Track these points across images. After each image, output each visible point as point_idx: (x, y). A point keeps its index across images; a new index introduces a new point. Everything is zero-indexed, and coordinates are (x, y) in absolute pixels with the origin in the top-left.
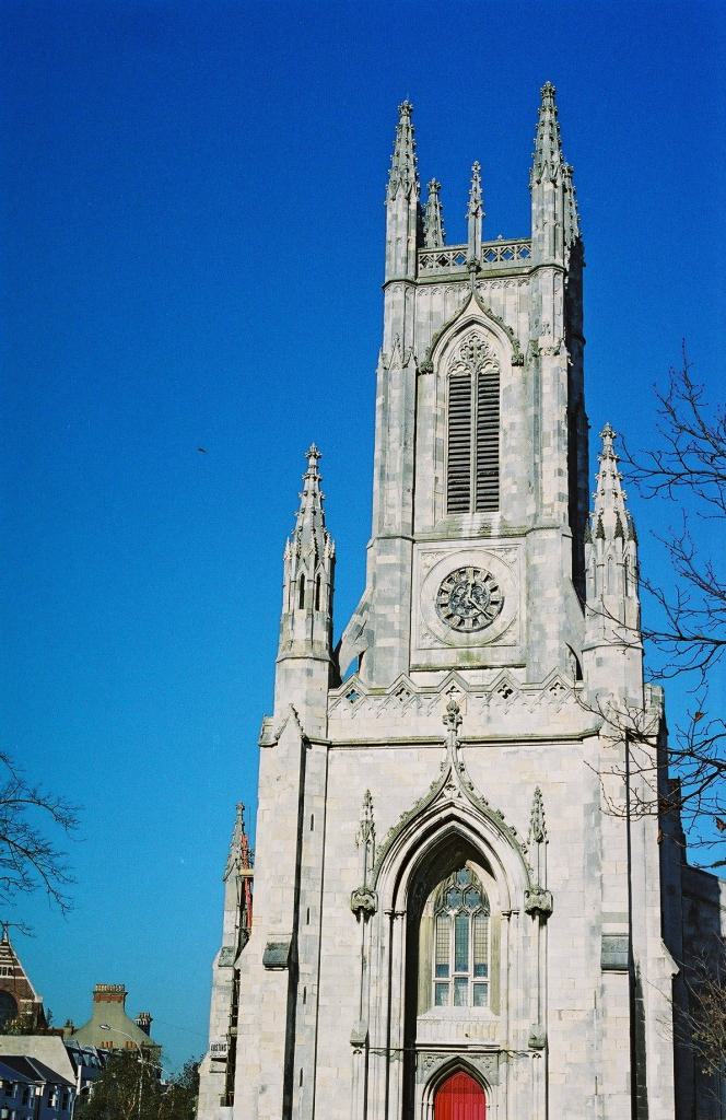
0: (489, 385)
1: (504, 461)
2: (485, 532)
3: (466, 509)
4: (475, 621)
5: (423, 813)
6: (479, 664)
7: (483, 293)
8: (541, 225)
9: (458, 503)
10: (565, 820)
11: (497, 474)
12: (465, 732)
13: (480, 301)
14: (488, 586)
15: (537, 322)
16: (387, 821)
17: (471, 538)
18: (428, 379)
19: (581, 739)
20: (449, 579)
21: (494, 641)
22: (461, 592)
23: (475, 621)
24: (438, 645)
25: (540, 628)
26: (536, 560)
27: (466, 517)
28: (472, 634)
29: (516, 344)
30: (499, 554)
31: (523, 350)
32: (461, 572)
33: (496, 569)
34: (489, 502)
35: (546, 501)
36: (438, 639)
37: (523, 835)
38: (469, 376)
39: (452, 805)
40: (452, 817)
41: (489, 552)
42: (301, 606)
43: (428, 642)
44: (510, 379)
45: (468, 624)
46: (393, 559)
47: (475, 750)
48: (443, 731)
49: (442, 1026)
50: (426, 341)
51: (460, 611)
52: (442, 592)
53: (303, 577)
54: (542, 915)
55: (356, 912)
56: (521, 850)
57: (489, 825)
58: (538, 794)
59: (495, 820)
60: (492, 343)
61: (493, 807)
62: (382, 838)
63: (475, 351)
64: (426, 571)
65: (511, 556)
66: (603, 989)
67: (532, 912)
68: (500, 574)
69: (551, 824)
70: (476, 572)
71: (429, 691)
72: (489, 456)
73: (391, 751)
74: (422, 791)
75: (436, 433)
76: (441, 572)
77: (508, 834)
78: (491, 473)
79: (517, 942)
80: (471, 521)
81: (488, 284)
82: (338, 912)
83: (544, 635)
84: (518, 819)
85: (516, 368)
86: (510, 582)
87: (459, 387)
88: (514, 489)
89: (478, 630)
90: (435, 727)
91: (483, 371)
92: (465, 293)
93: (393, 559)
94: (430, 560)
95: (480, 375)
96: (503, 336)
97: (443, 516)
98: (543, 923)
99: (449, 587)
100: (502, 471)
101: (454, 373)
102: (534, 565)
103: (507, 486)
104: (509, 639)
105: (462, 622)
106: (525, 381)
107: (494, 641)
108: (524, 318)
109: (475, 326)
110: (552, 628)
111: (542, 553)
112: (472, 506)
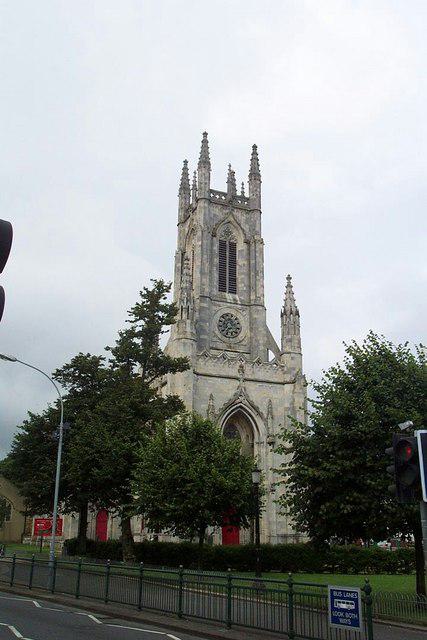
0: (233, 247)
5: (231, 404)
9: (222, 288)
16: (219, 404)
19: (284, 384)
20: (222, 317)
34: (233, 291)
40: (241, 407)
44: (241, 246)
56: (265, 421)
59: (256, 409)
61: (255, 404)
62: (217, 412)
63: (228, 233)
69: (275, 413)
71: (233, 359)
72: (233, 273)
73: (219, 379)
74: (230, 394)
75: (216, 260)
76: (219, 314)
77: (260, 414)
78: (233, 280)
80: (229, 296)
84: (263, 410)
87: (222, 245)
90: (234, 372)
93: (205, 305)
96: (241, 231)
103: (241, 286)
106: (249, 250)
108: (247, 226)
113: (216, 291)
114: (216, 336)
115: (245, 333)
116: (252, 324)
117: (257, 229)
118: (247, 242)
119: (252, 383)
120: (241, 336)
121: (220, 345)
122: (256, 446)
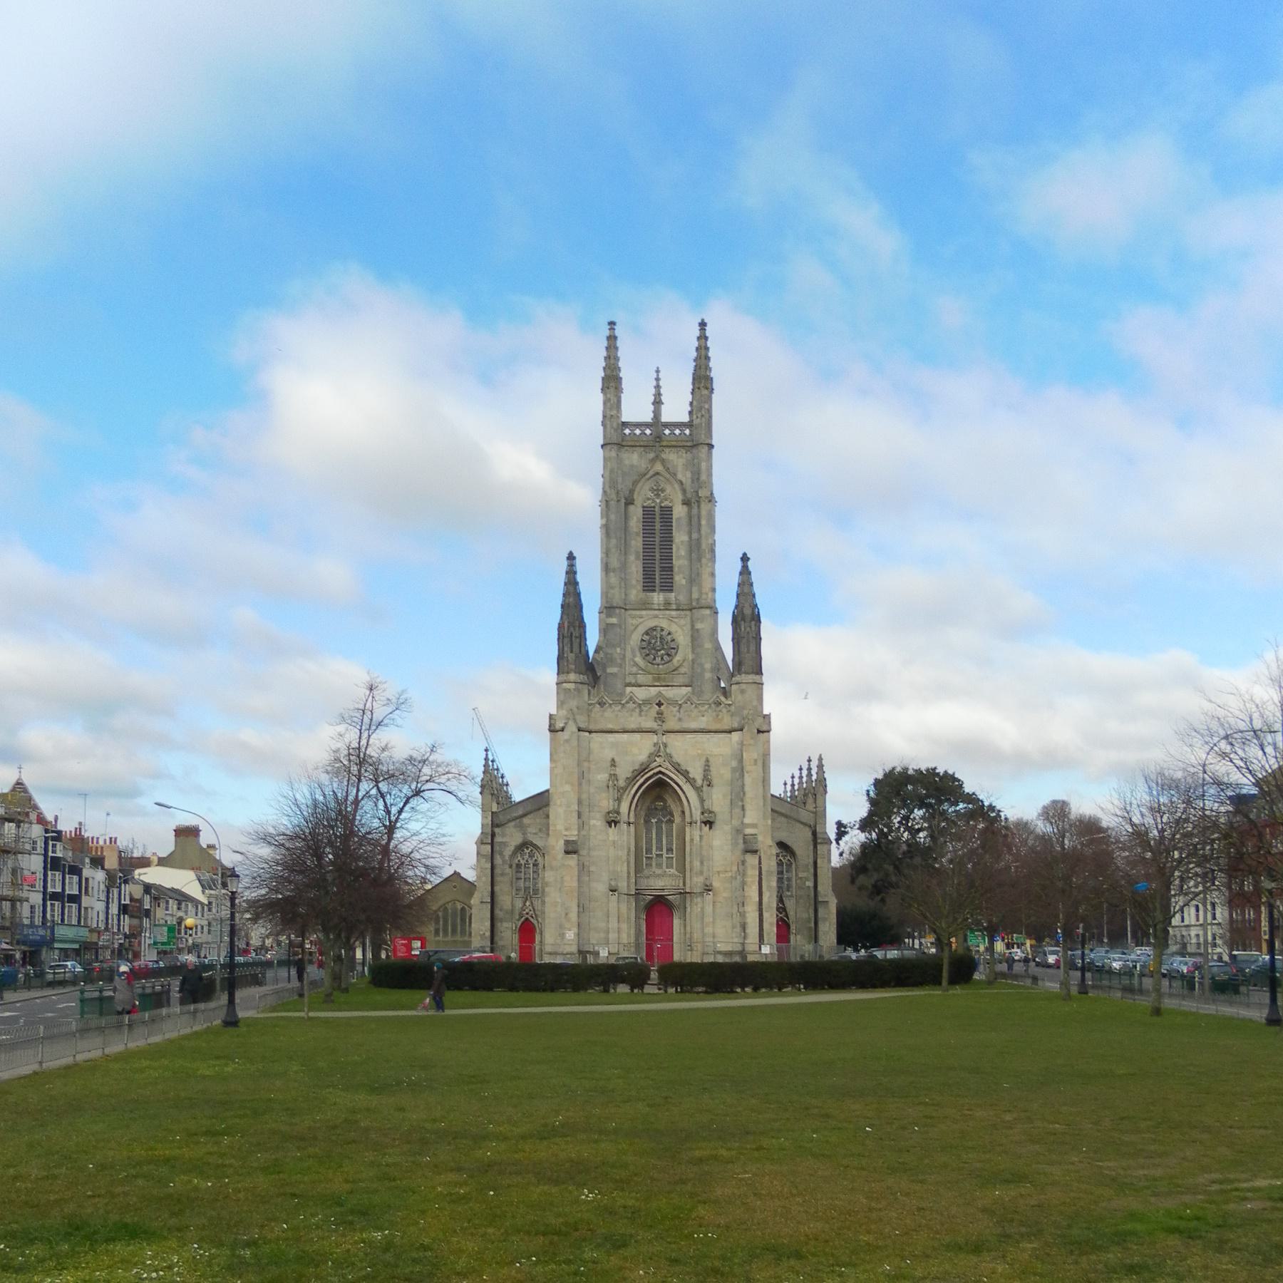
0: (667, 513)
1: (676, 563)
2: (667, 606)
3: (654, 591)
4: (662, 659)
5: (643, 769)
6: (664, 684)
7: (663, 456)
8: (699, 416)
9: (649, 586)
10: (722, 774)
11: (672, 571)
12: (665, 727)
13: (663, 462)
14: (669, 637)
15: (698, 479)
16: (624, 772)
17: (660, 610)
18: (631, 508)
20: (647, 633)
21: (673, 671)
22: (653, 641)
23: (662, 659)
24: (640, 672)
25: (701, 665)
26: (699, 626)
27: (655, 594)
28: (661, 666)
29: (684, 491)
30: (676, 620)
31: (689, 495)
32: (654, 629)
33: (674, 628)
34: (668, 586)
35: (704, 591)
36: (642, 670)
37: (699, 782)
38: (654, 507)
39: (660, 766)
40: (660, 772)
41: (670, 619)
42: (572, 652)
43: (634, 669)
44: (679, 511)
45: (658, 660)
46: (614, 620)
47: (672, 735)
48: (654, 725)
49: (662, 881)
50: (629, 484)
51: (653, 652)
52: (643, 640)
53: (572, 633)
54: (710, 823)
55: (609, 824)
56: (698, 790)
57: (681, 777)
58: (707, 761)
59: (685, 774)
60: (669, 489)
62: (622, 783)
63: (658, 491)
64: (633, 628)
65: (682, 622)
66: (743, 862)
67: (705, 823)
68: (676, 632)
70: (662, 630)
72: (668, 557)
73: (625, 736)
74: (643, 757)
75: (637, 543)
76: (642, 629)
79: (697, 838)
80: (658, 598)
81: (667, 450)
82: (597, 822)
83: (703, 670)
84: (696, 773)
85: (685, 506)
86: (682, 637)
87: (648, 513)
88: (684, 582)
89: (663, 664)
91: (663, 505)
92: (652, 455)
94: (634, 622)
95: (661, 507)
97: (642, 595)
98: (710, 828)
99: (646, 638)
100: (676, 569)
101: (645, 504)
102: (698, 630)
103: (680, 580)
104: (682, 670)
105: (654, 659)
107: (673, 671)
108: (689, 475)
109: (658, 476)
110: (708, 666)
111: (701, 622)
112: (657, 589)
113: (635, 593)
114: (636, 664)
115: (684, 653)
116: (695, 636)
117: (703, 477)
118: (687, 503)
119: (679, 736)
120: (677, 659)
121: (642, 679)
122: (687, 829)
